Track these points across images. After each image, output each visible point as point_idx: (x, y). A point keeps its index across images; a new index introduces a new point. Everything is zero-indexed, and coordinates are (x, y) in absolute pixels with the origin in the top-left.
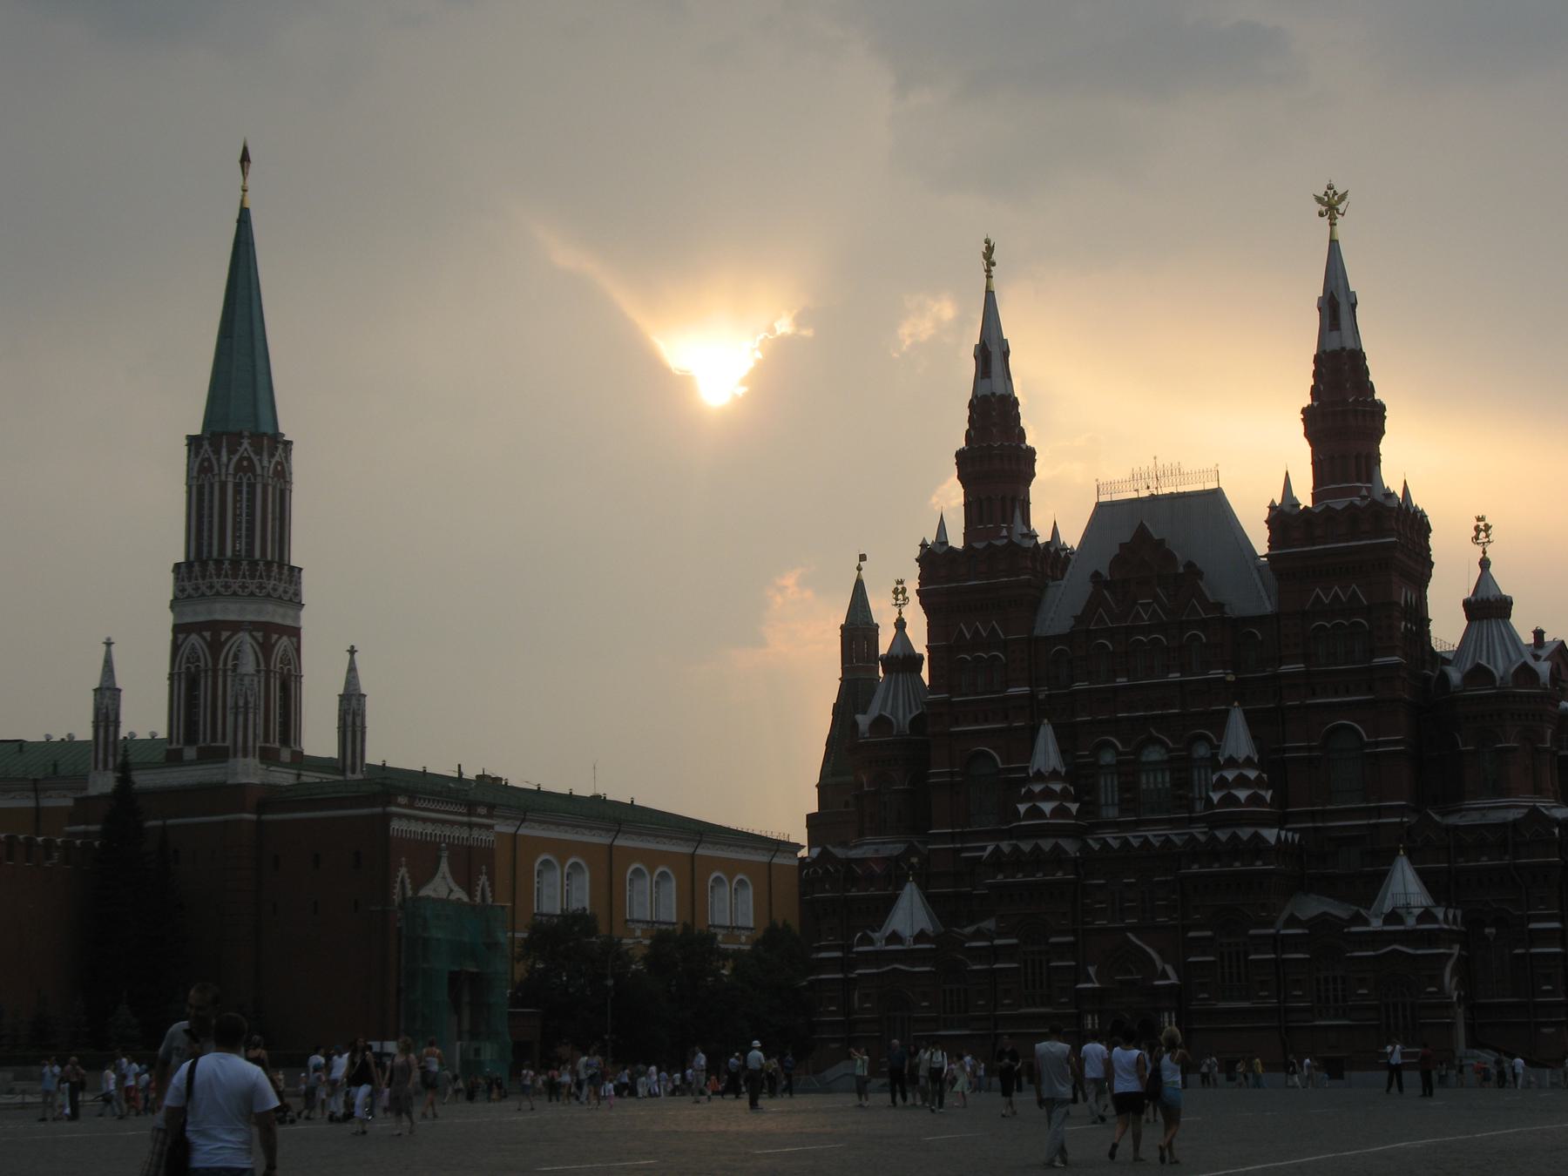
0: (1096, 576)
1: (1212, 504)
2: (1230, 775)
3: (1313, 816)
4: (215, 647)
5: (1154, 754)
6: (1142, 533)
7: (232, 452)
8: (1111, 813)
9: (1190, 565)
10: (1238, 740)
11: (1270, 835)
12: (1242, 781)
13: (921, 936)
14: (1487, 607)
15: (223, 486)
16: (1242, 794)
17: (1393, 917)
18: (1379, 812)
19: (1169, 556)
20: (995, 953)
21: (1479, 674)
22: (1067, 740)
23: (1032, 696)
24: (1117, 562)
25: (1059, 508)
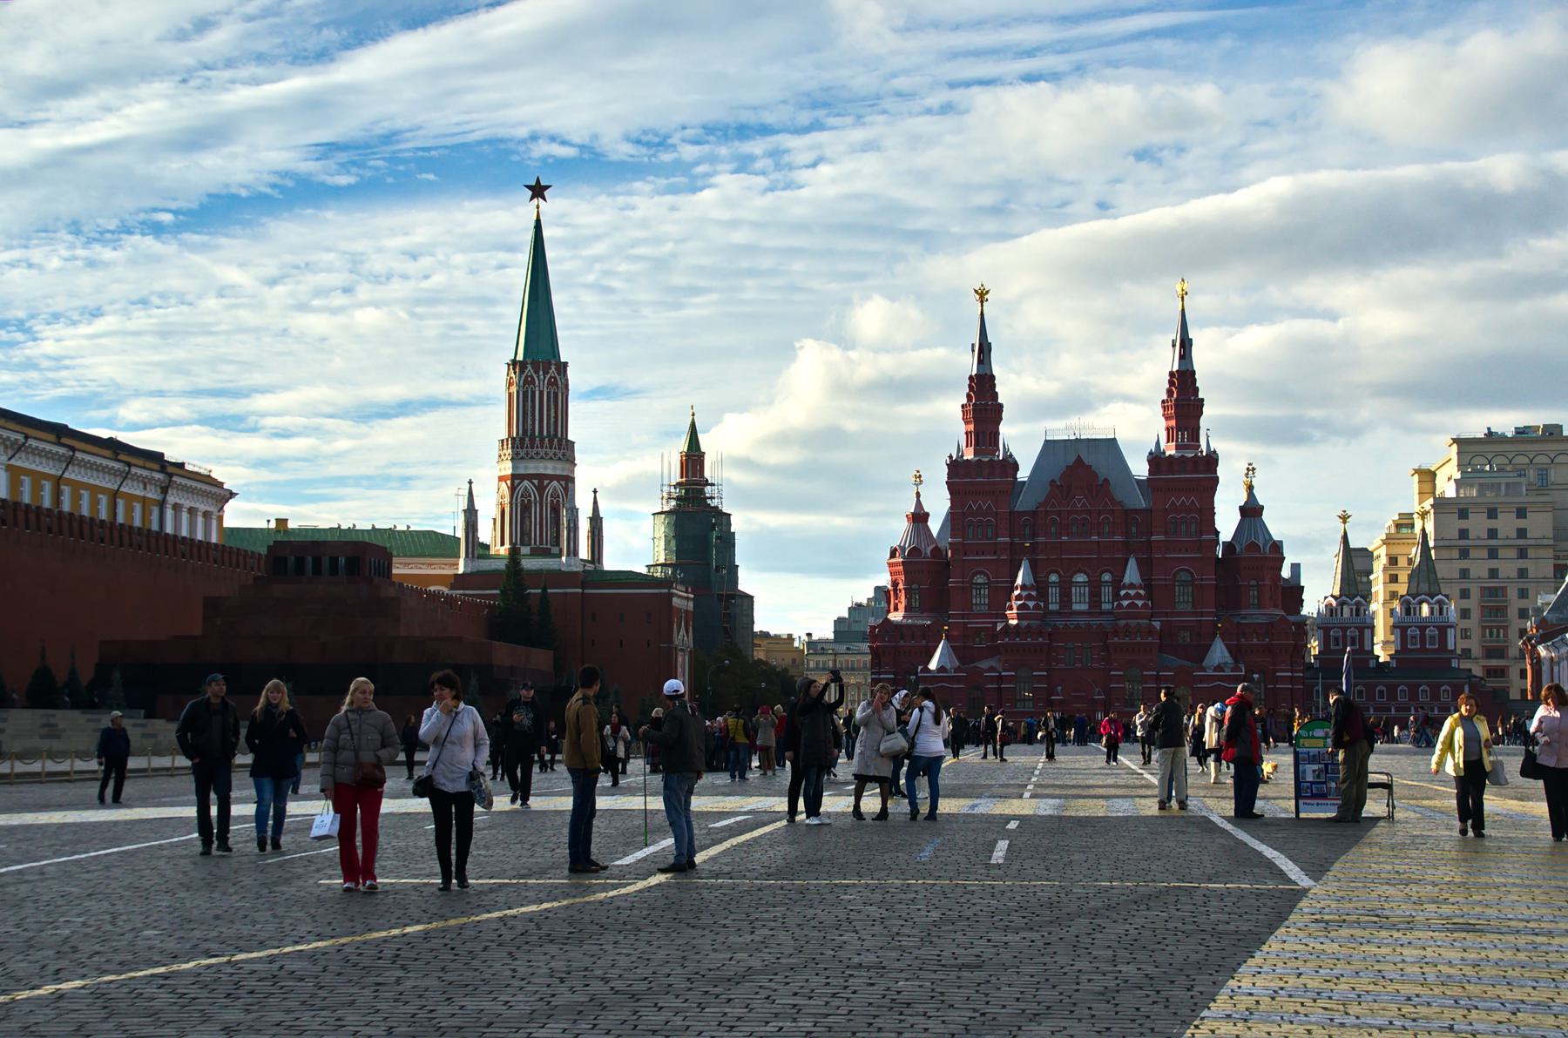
0: (1053, 481)
1: (1110, 446)
2: (1132, 592)
3: (1166, 615)
4: (541, 489)
5: (1081, 578)
6: (1079, 460)
7: (545, 373)
8: (1051, 607)
9: (1106, 480)
10: (1132, 574)
11: (1157, 624)
12: (1138, 596)
13: (956, 670)
14: (1251, 511)
15: (541, 393)
16: (1140, 603)
17: (1219, 668)
18: (1202, 614)
19: (1095, 475)
20: (1000, 679)
21: (1253, 546)
22: (1034, 567)
23: (1012, 543)
24: (1063, 476)
25: (1022, 441)
